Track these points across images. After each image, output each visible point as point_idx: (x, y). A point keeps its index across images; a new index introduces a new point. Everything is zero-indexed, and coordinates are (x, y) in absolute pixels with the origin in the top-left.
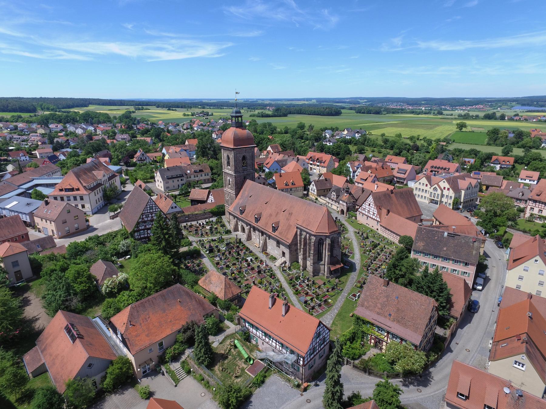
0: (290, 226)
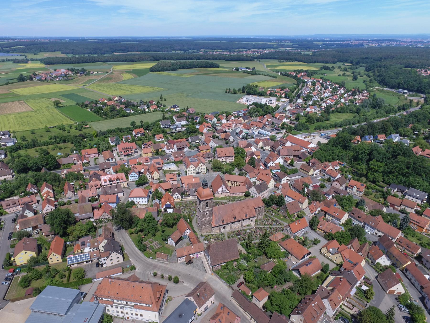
0: (251, 210)
